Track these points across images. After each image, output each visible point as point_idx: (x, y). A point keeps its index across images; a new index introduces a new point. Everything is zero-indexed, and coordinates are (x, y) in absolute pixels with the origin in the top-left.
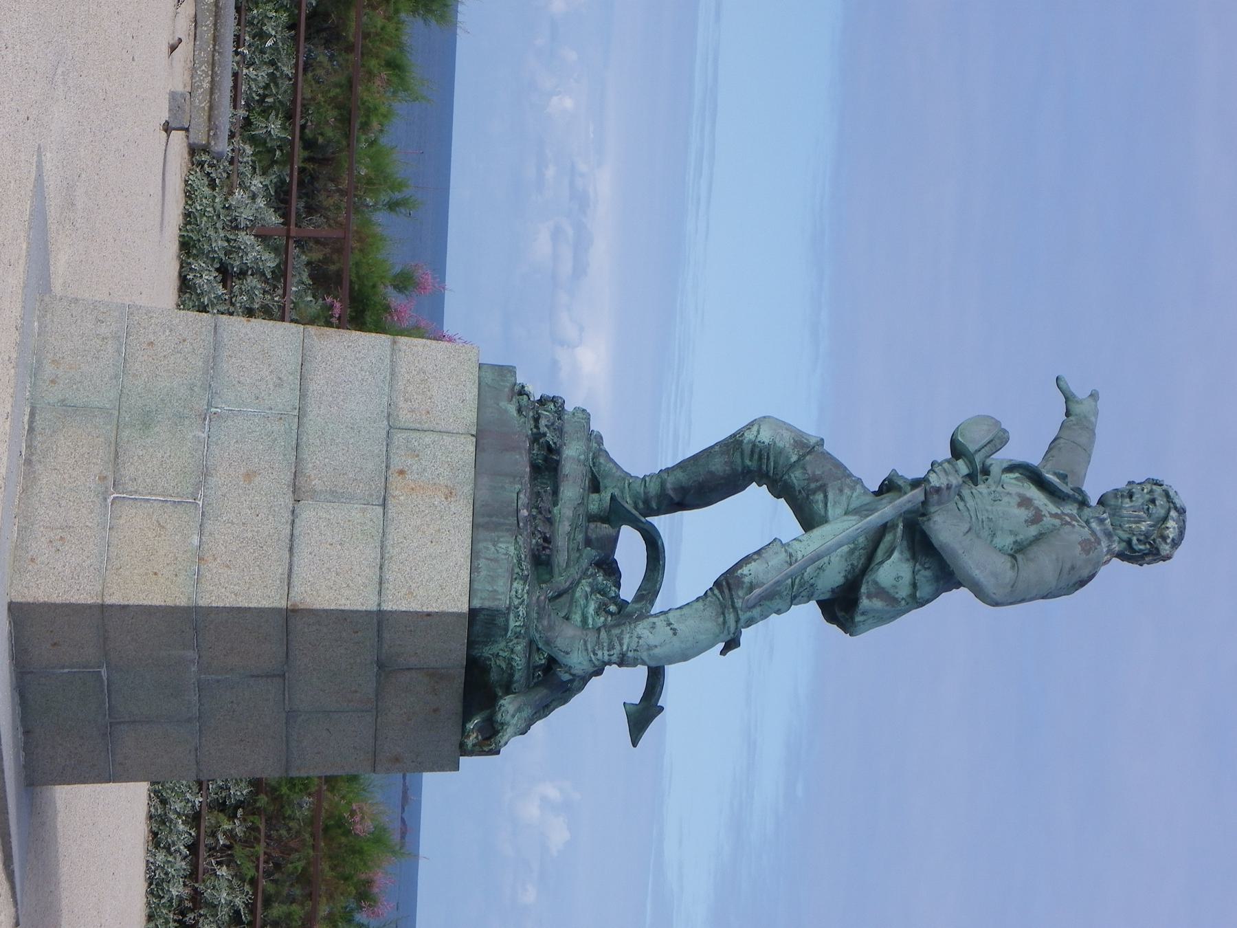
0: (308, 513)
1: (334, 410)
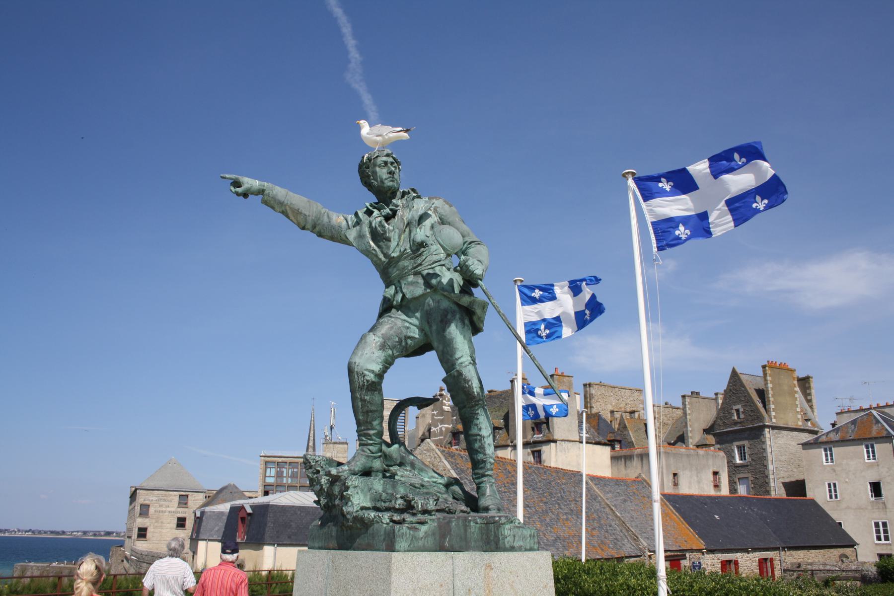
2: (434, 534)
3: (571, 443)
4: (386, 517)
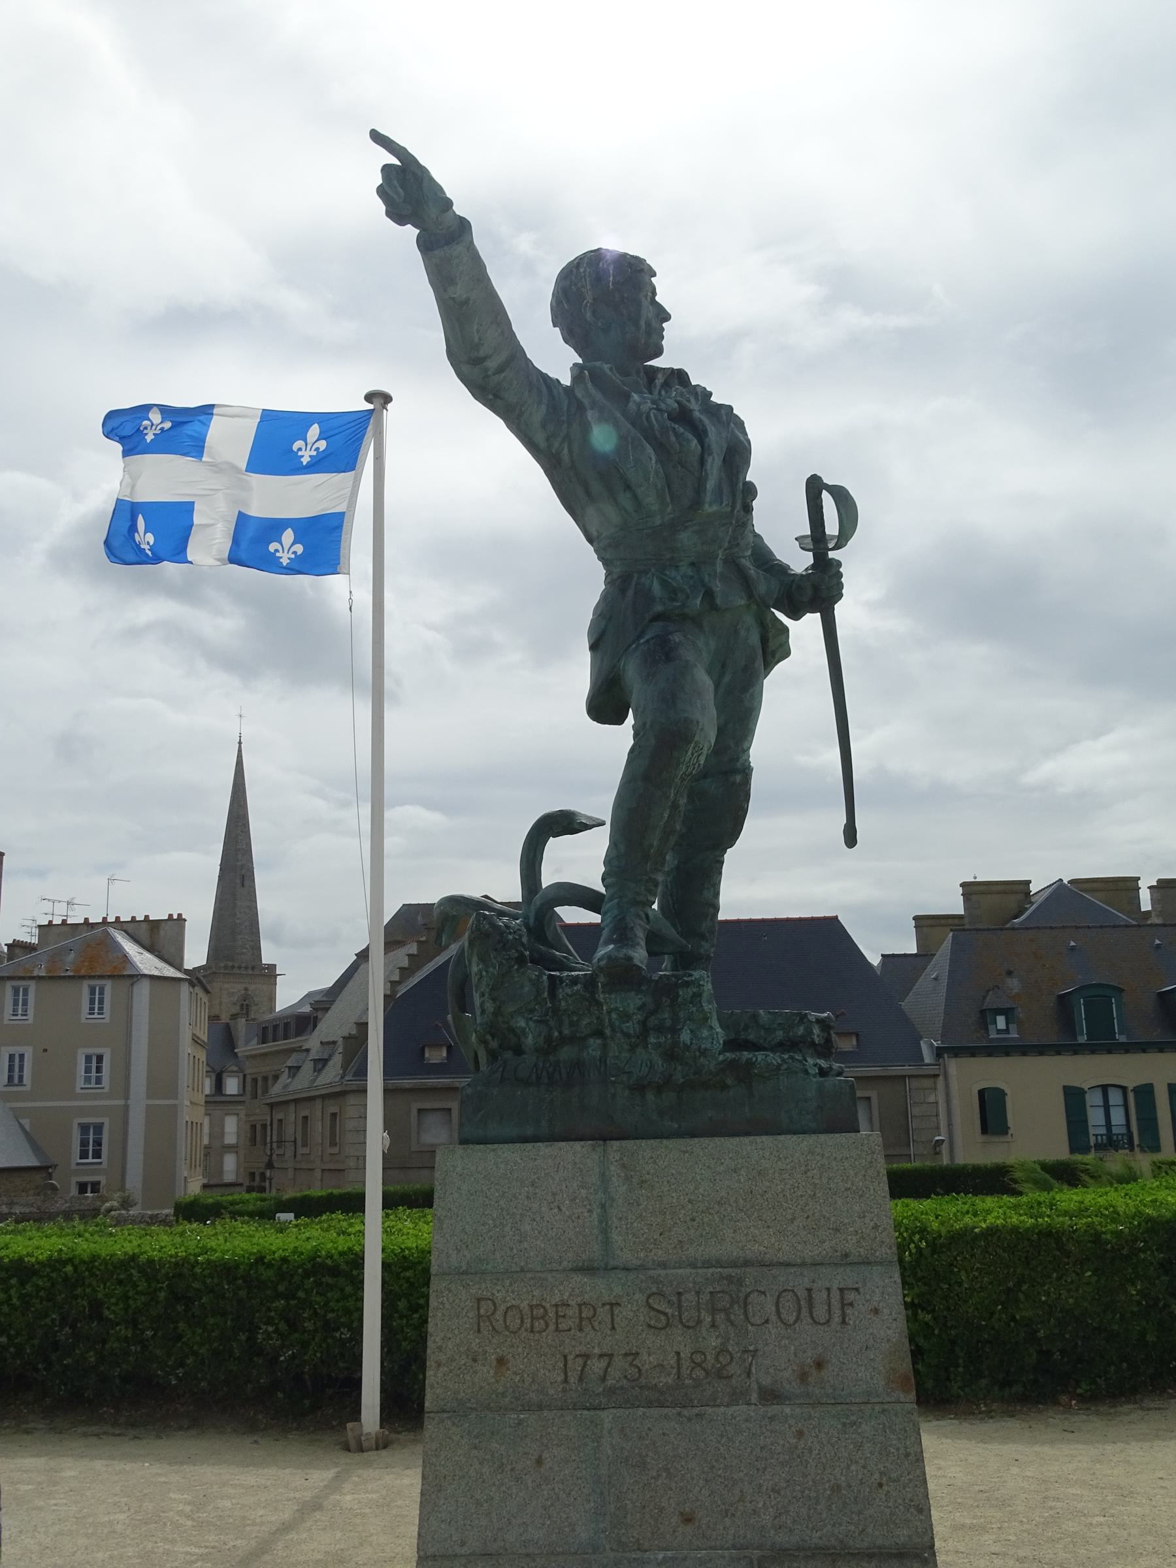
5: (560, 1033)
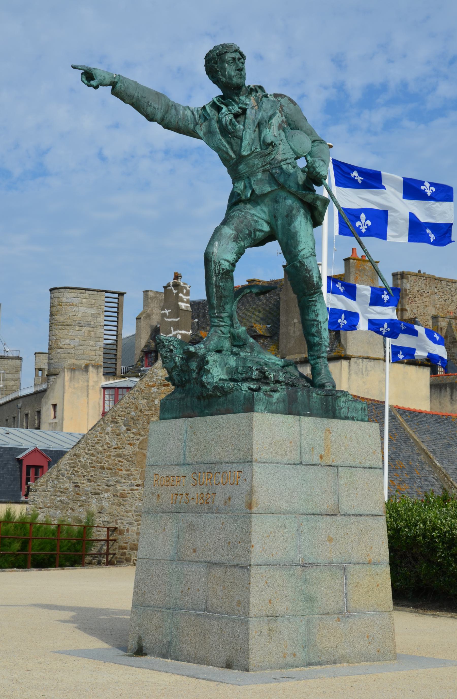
0: (345, 507)
1: (295, 494)
2: (284, 401)
3: (372, 363)
4: (245, 386)
5: (185, 379)
